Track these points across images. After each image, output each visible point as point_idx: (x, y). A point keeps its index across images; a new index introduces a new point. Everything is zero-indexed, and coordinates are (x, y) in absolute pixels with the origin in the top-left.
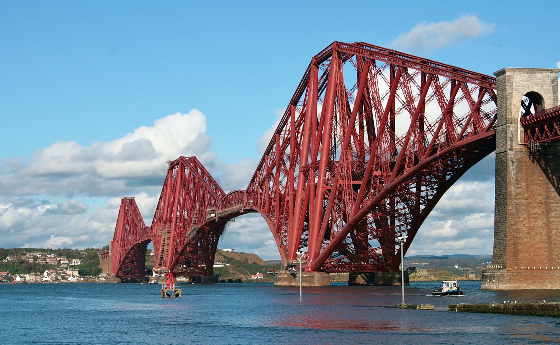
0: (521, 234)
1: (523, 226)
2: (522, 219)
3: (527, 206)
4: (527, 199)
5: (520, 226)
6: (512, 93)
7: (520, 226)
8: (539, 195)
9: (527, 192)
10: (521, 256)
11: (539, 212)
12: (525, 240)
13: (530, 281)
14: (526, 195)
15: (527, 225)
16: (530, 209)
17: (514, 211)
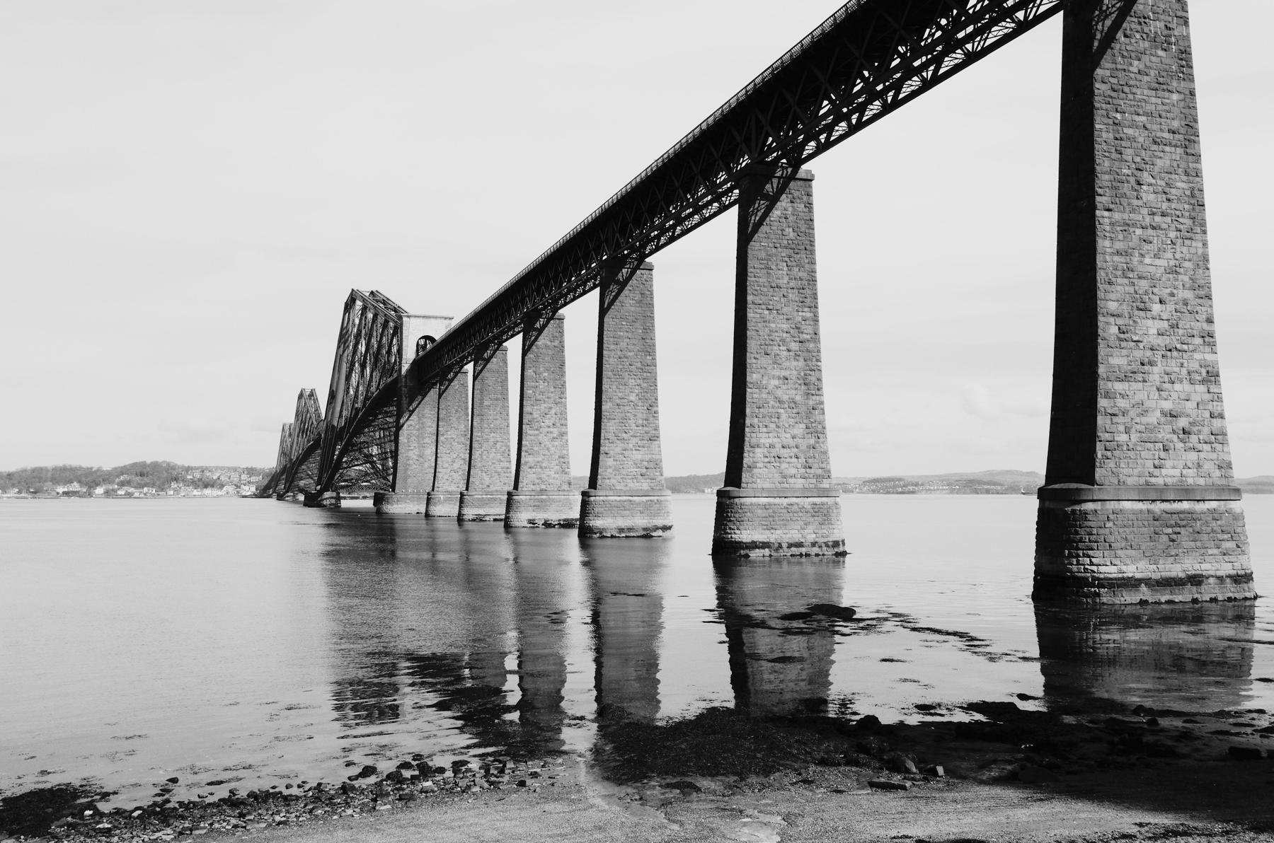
0: (411, 461)
1: (413, 454)
2: (412, 448)
3: (418, 436)
4: (418, 430)
5: (410, 454)
6: (407, 336)
7: (410, 454)
8: (429, 427)
9: (419, 423)
10: (409, 480)
11: (430, 442)
12: (415, 466)
13: (416, 503)
14: (417, 427)
15: (416, 453)
16: (421, 439)
17: (406, 441)
